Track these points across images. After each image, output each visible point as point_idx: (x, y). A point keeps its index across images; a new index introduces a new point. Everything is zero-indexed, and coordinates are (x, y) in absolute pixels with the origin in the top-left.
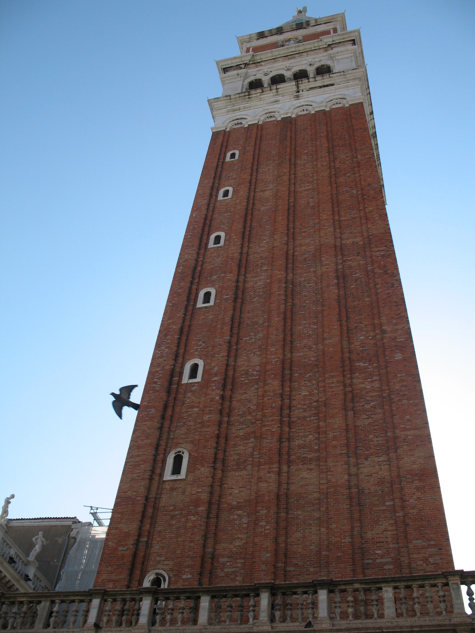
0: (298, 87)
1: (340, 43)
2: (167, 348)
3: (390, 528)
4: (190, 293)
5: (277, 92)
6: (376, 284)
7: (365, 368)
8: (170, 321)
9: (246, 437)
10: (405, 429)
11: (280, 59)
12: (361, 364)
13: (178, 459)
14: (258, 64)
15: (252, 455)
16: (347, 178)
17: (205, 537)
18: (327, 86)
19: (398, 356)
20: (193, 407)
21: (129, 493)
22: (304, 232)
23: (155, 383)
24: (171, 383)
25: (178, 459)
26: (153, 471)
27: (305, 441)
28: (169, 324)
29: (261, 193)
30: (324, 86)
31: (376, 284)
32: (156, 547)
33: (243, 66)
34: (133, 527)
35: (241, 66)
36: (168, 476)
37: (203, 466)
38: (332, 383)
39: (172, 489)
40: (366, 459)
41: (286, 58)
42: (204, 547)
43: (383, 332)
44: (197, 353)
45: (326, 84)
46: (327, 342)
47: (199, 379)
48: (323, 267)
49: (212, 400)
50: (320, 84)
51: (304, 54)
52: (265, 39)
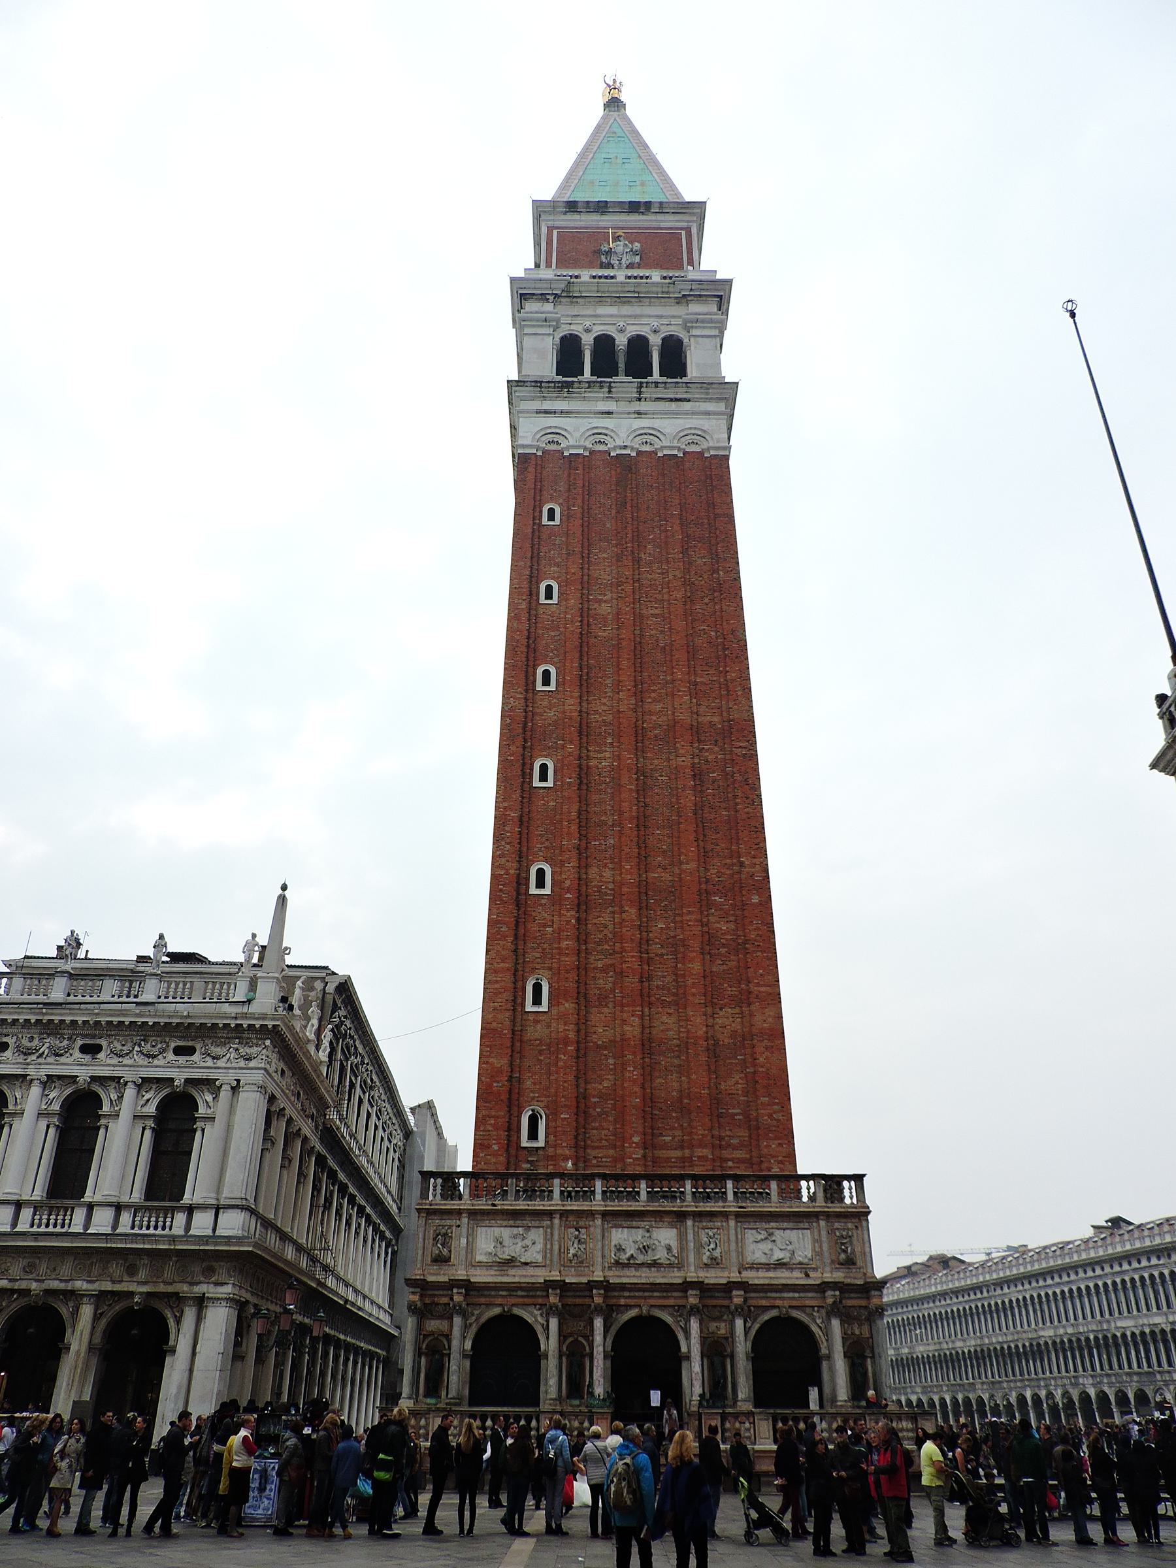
0: (640, 393)
1: (700, 296)
2: (508, 843)
3: (740, 1081)
4: (524, 764)
5: (610, 392)
6: (735, 797)
7: (721, 904)
8: (506, 804)
9: (605, 970)
10: (758, 985)
11: (609, 300)
12: (717, 898)
13: (537, 988)
14: (575, 300)
15: (613, 991)
16: (705, 607)
17: (577, 1078)
18: (680, 400)
19: (755, 899)
20: (545, 926)
21: (494, 1025)
22: (654, 691)
23: (501, 890)
24: (518, 894)
25: (537, 988)
26: (514, 1001)
27: (663, 982)
28: (505, 808)
29: (596, 605)
30: (677, 400)
31: (735, 797)
32: (529, 1083)
33: (551, 298)
34: (502, 1062)
35: (548, 297)
36: (529, 1007)
37: (567, 1001)
38: (690, 921)
39: (537, 1022)
40: (721, 1009)
41: (618, 300)
42: (577, 1086)
43: (742, 864)
44: (541, 854)
45: (678, 396)
46: (684, 867)
47: (547, 890)
48: (678, 759)
49: (568, 922)
50: (672, 396)
51: (645, 300)
52: (576, 216)
